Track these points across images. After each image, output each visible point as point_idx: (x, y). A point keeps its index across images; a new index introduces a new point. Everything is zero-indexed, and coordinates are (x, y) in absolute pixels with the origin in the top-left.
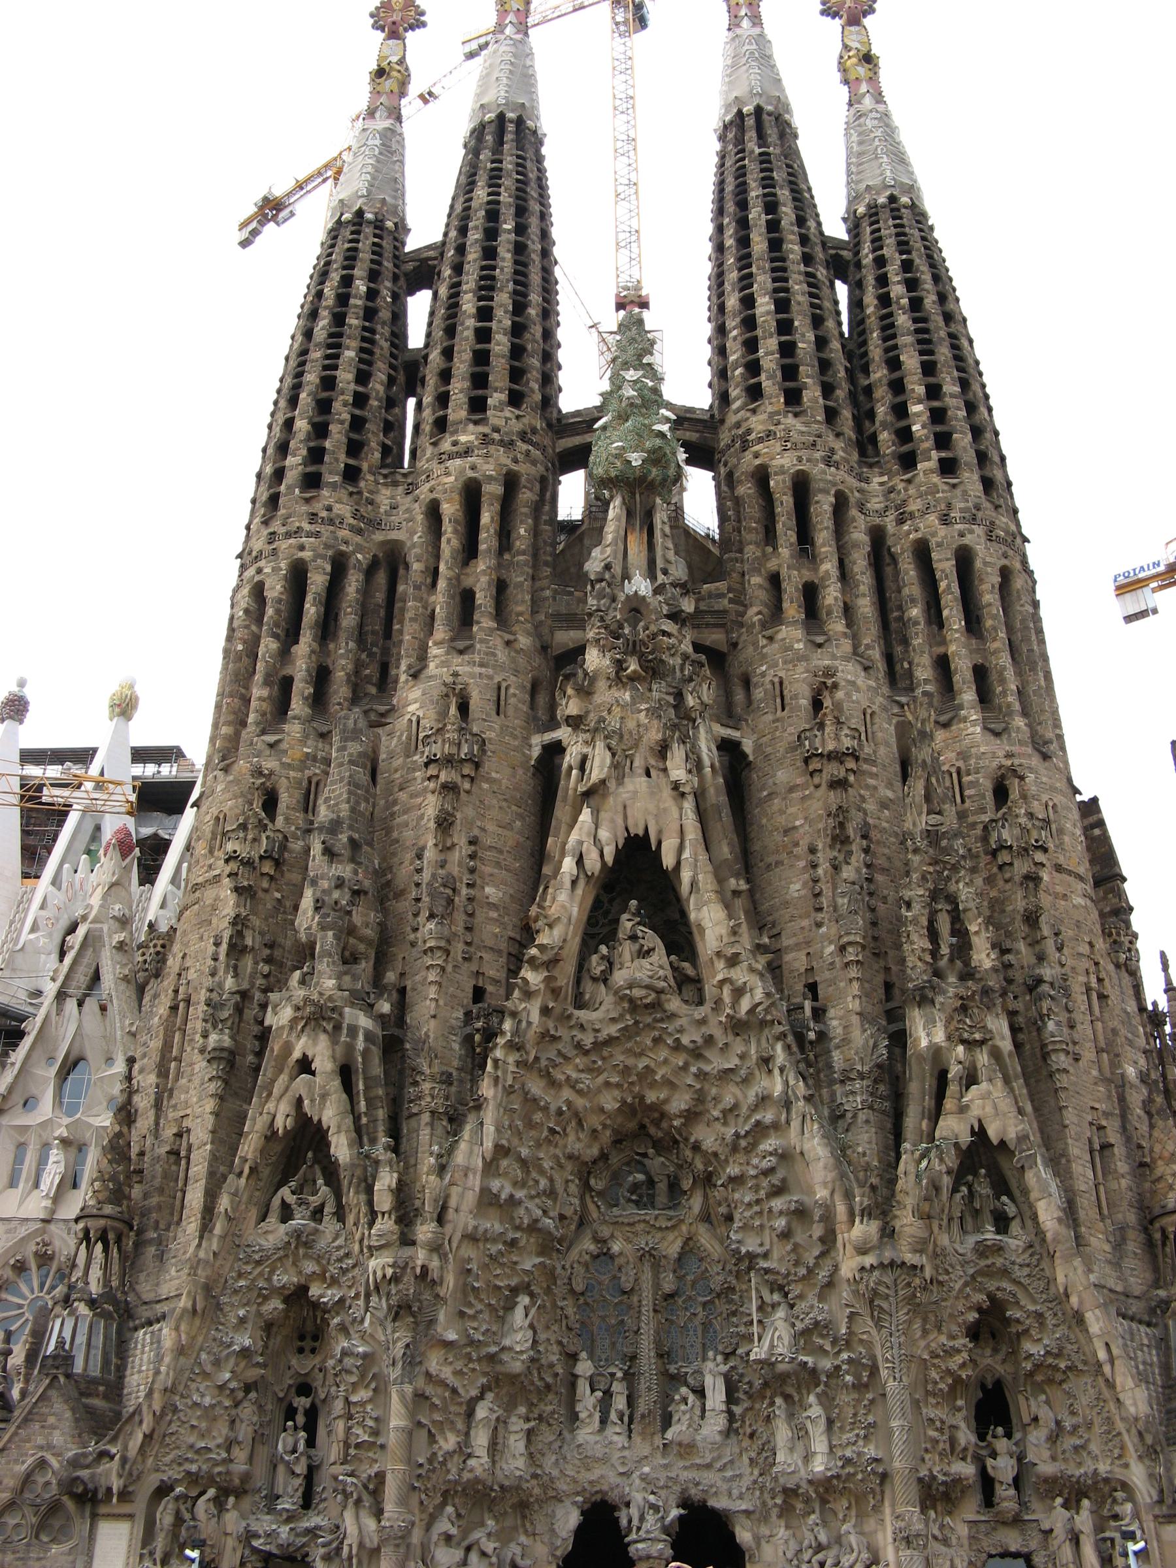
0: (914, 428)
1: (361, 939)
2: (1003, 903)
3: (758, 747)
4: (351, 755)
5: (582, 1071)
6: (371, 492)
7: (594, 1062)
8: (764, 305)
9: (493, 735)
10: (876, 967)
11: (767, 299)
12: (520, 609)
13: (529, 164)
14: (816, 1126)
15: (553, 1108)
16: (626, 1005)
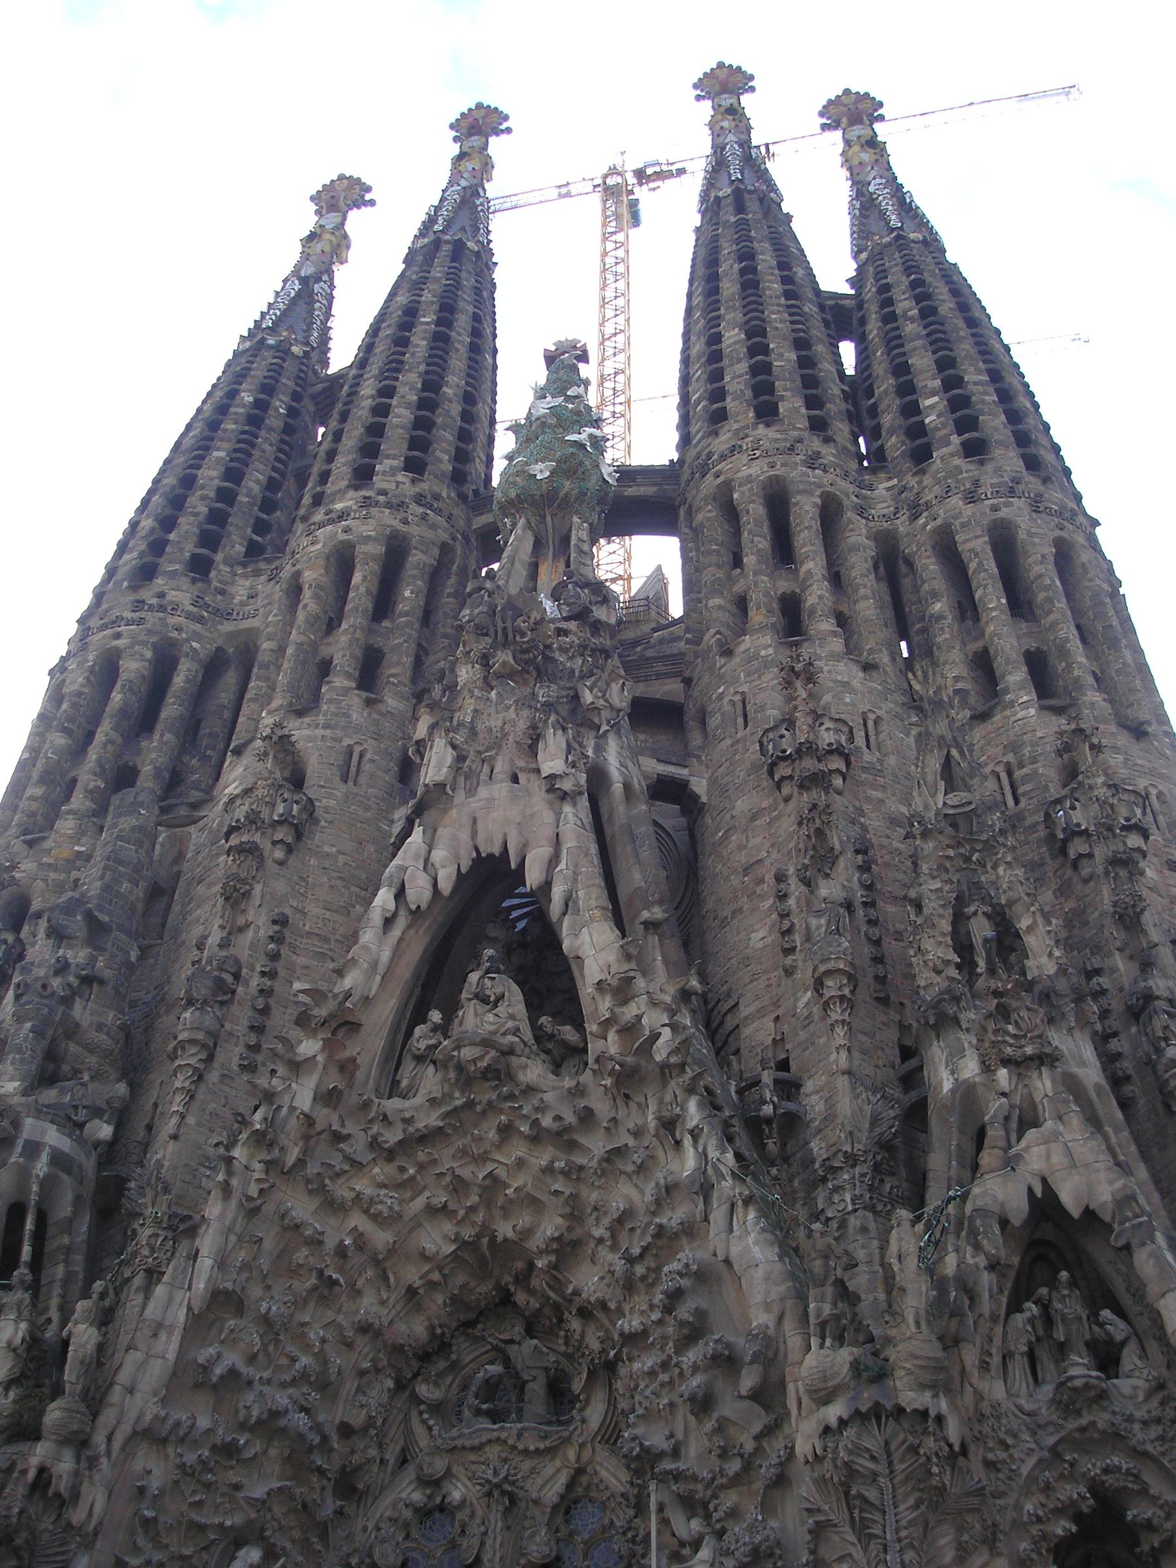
0: (927, 421)
1: (91, 1049)
2: (1084, 912)
3: (712, 782)
4: (122, 831)
5: (384, 1186)
6: (219, 582)
7: (402, 1169)
8: (733, 337)
9: (332, 803)
10: (883, 1018)
11: (737, 330)
12: (393, 671)
13: (464, 275)
14: (752, 1215)
15: (330, 1243)
16: (452, 1075)
